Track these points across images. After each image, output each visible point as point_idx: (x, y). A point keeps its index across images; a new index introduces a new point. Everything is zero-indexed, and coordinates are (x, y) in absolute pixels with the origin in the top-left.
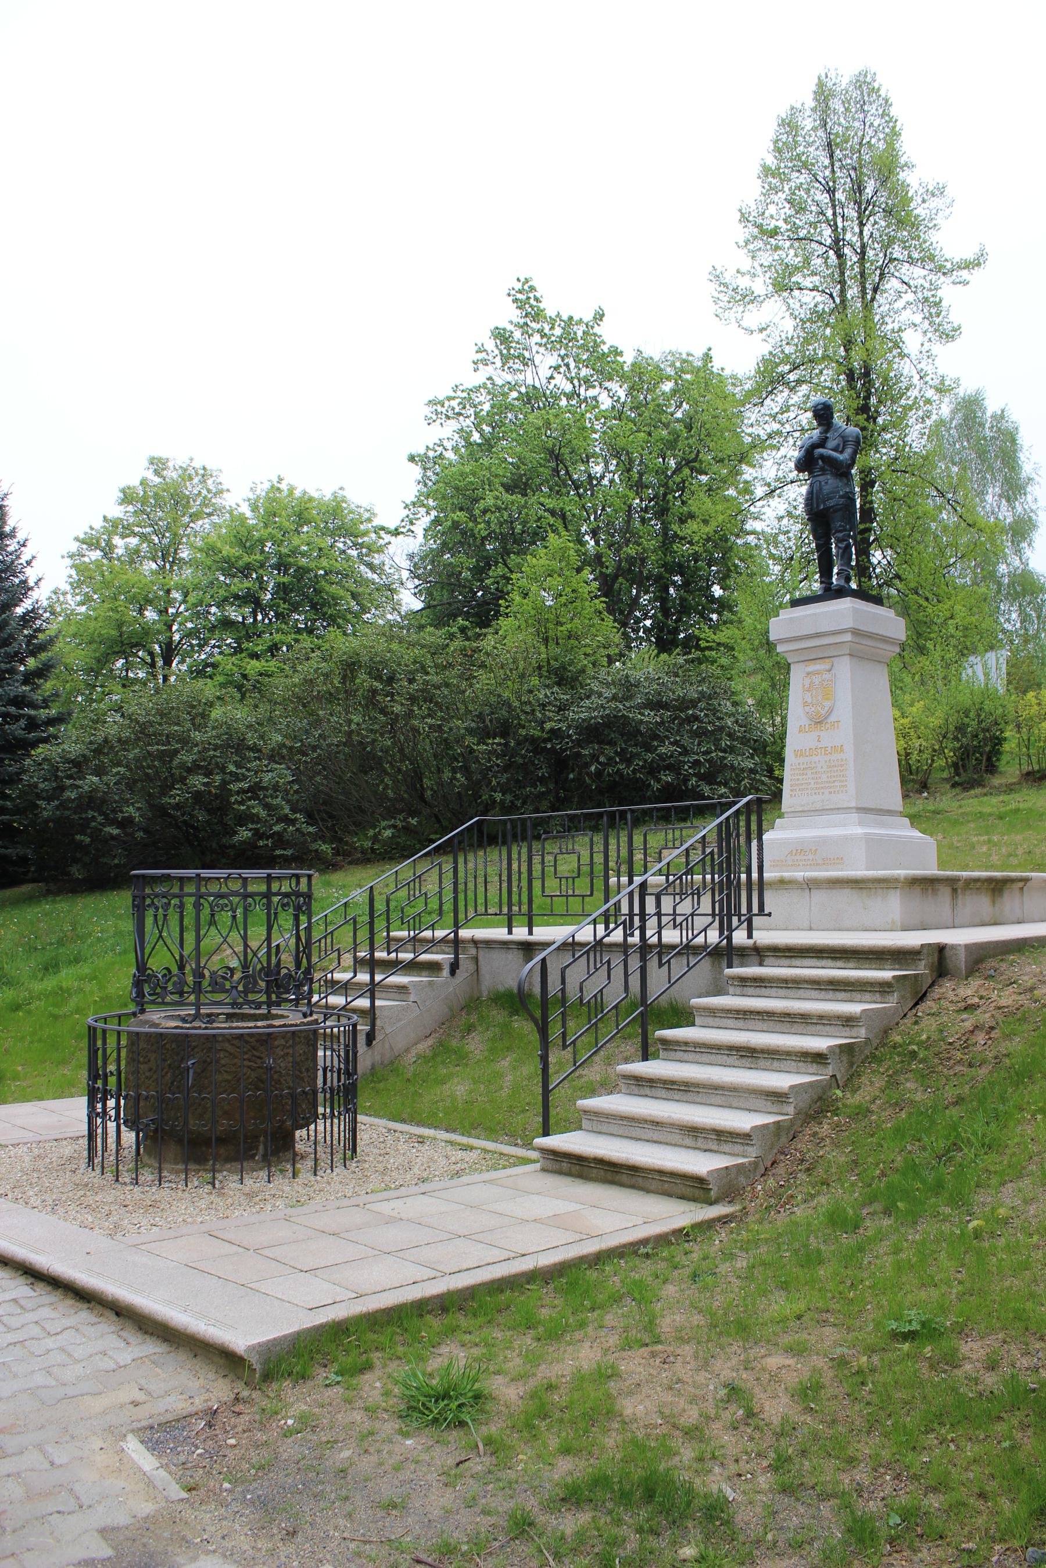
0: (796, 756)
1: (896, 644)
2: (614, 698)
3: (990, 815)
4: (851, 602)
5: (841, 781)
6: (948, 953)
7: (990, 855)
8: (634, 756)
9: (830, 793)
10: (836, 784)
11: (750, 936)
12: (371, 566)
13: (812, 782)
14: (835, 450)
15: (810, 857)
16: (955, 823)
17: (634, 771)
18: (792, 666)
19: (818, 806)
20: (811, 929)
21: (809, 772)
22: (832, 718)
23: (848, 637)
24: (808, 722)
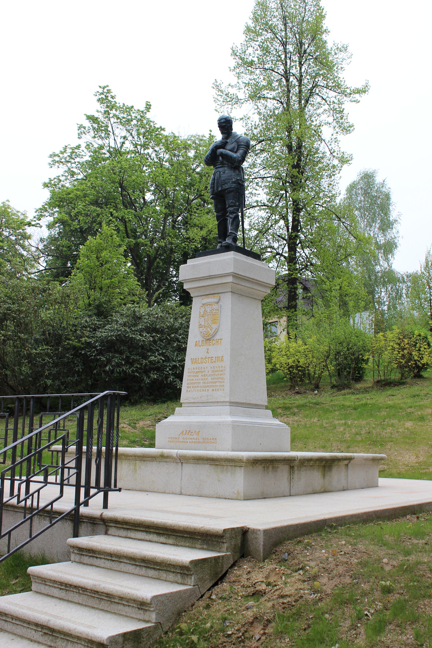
0: (192, 363)
2: (125, 325)
3: (349, 407)
4: (234, 254)
5: (220, 382)
6: (250, 536)
7: (344, 434)
8: (134, 361)
9: (213, 390)
10: (217, 384)
11: (105, 506)
12: (23, 247)
13: (202, 382)
14: (231, 150)
15: (195, 437)
16: (327, 411)
17: (133, 371)
18: (194, 299)
19: (204, 399)
20: (181, 494)
21: (200, 375)
22: (217, 337)
23: (230, 279)
24: (201, 339)
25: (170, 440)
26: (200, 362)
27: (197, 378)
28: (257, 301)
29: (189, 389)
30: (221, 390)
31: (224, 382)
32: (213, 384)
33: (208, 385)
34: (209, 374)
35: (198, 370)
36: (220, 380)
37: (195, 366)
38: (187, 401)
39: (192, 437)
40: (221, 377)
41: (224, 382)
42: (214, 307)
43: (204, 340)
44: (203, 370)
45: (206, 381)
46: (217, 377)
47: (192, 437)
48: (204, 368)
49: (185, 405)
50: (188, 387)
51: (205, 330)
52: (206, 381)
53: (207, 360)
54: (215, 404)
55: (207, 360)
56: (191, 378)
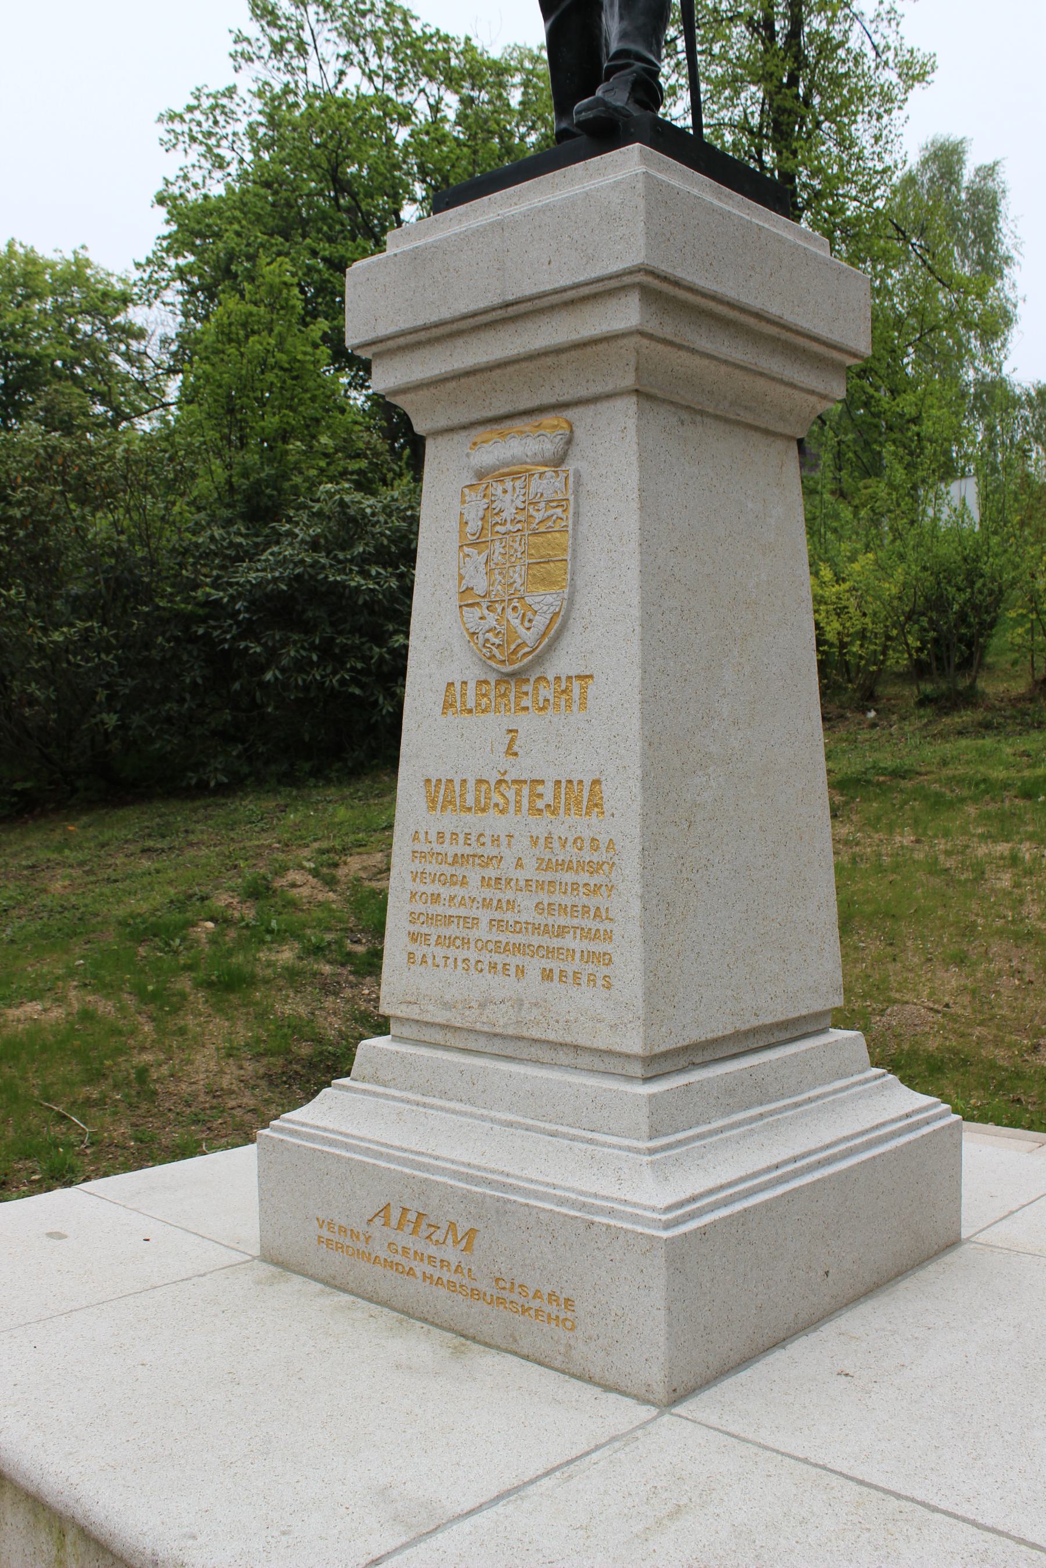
1: (836, 367)
2: (314, 545)
3: (1006, 786)
4: (645, 159)
7: (1021, 901)
8: (346, 650)
9: (547, 975)
10: (570, 942)
12: (128, 358)
13: (485, 916)
15: (451, 1254)
16: (937, 803)
17: (343, 682)
18: (431, 450)
19: (502, 1019)
21: (474, 876)
24: (474, 673)
26: (470, 800)
27: (457, 891)
28: (780, 445)
29: (420, 950)
30: (592, 980)
31: (608, 936)
32: (546, 941)
33: (519, 939)
34: (521, 875)
35: (461, 849)
36: (588, 923)
37: (448, 821)
38: (413, 1012)
39: (432, 1250)
40: (593, 902)
41: (608, 936)
42: (536, 485)
43: (492, 678)
44: (489, 851)
45: (509, 917)
46: (567, 900)
47: (432, 1250)
48: (496, 840)
49: (407, 1031)
50: (414, 937)
51: (491, 620)
52: (509, 917)
53: (510, 794)
54: (562, 1057)
55: (510, 794)
56: (431, 889)
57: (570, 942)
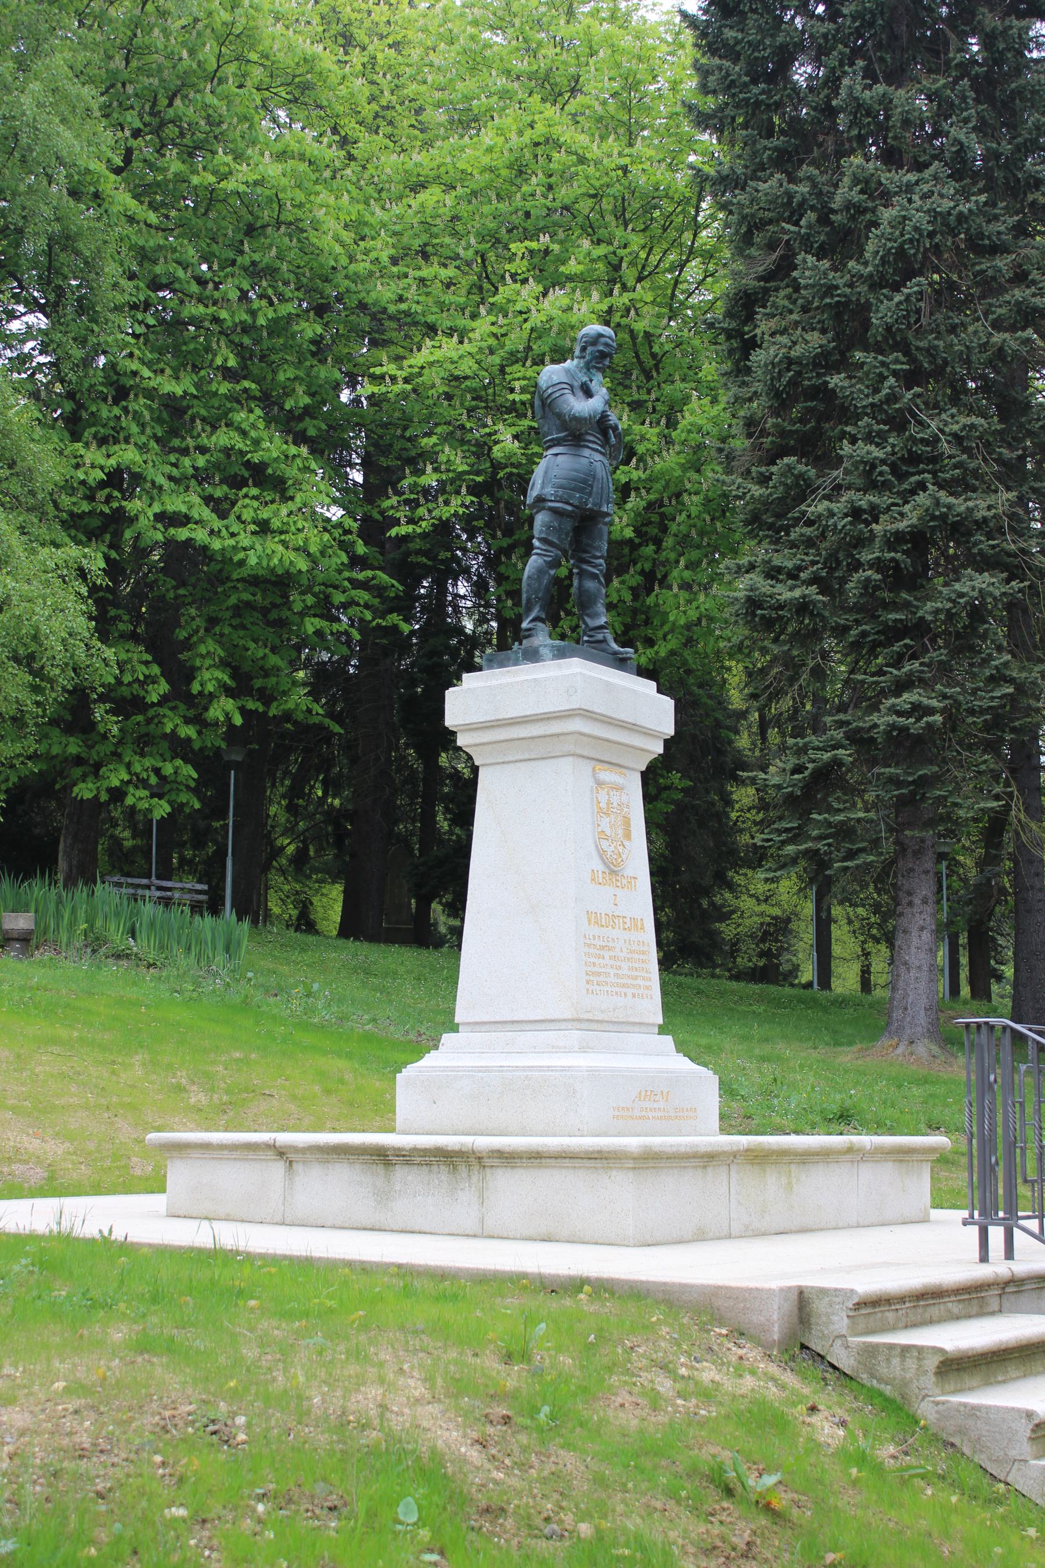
13: (612, 972)
25: (616, 1113)
29: (591, 988)
44: (611, 944)
54: (636, 1029)
56: (592, 960)
57: (639, 982)
